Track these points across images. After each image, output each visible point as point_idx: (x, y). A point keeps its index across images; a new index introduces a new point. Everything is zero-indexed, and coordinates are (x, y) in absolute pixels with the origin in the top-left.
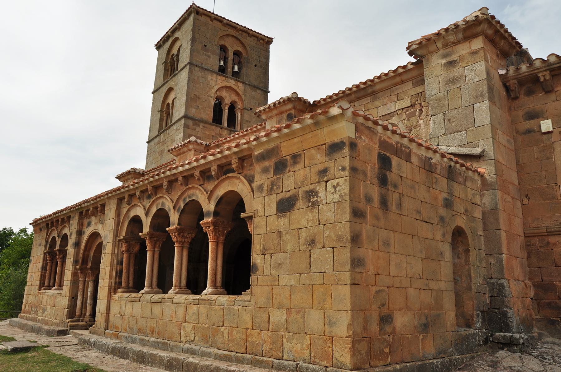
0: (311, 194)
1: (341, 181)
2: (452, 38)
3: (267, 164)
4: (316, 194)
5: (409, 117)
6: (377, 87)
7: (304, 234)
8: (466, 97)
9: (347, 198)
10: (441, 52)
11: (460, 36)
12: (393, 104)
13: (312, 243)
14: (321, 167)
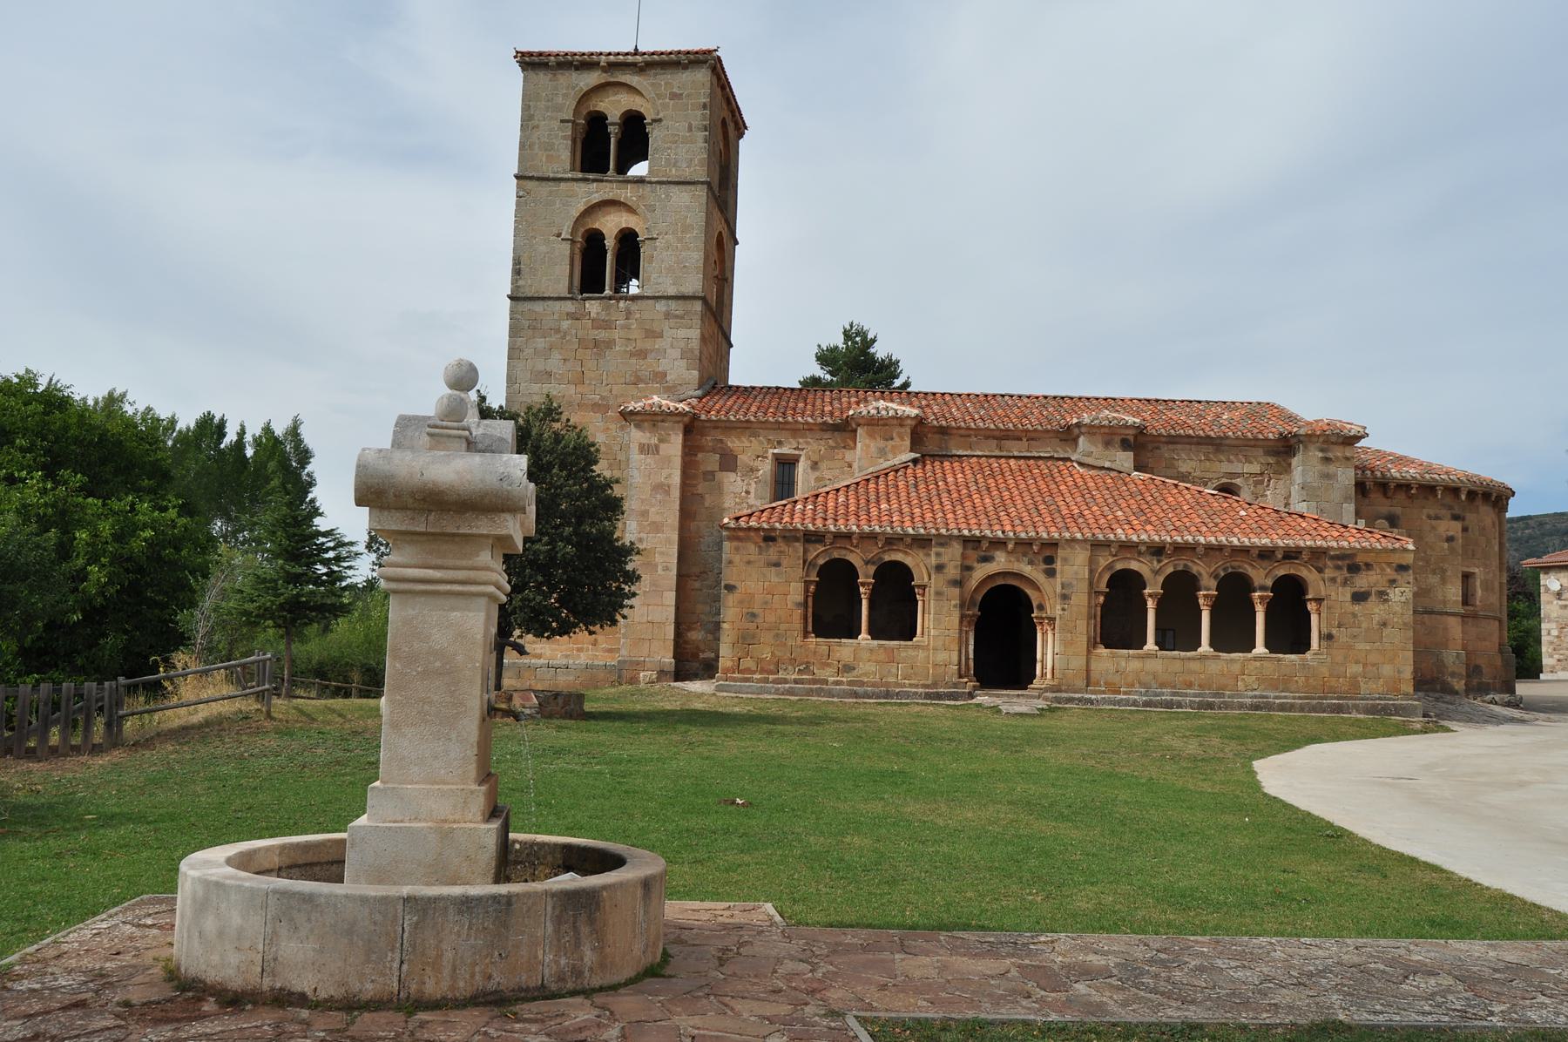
0: (1381, 594)
1: (1407, 590)
2: (1333, 439)
3: (1340, 563)
4: (1387, 594)
5: (1257, 483)
6: (1227, 442)
7: (1376, 619)
8: (1336, 496)
9: (1411, 601)
10: (1318, 444)
11: (1341, 440)
12: (1240, 465)
13: (1384, 624)
14: (1392, 578)
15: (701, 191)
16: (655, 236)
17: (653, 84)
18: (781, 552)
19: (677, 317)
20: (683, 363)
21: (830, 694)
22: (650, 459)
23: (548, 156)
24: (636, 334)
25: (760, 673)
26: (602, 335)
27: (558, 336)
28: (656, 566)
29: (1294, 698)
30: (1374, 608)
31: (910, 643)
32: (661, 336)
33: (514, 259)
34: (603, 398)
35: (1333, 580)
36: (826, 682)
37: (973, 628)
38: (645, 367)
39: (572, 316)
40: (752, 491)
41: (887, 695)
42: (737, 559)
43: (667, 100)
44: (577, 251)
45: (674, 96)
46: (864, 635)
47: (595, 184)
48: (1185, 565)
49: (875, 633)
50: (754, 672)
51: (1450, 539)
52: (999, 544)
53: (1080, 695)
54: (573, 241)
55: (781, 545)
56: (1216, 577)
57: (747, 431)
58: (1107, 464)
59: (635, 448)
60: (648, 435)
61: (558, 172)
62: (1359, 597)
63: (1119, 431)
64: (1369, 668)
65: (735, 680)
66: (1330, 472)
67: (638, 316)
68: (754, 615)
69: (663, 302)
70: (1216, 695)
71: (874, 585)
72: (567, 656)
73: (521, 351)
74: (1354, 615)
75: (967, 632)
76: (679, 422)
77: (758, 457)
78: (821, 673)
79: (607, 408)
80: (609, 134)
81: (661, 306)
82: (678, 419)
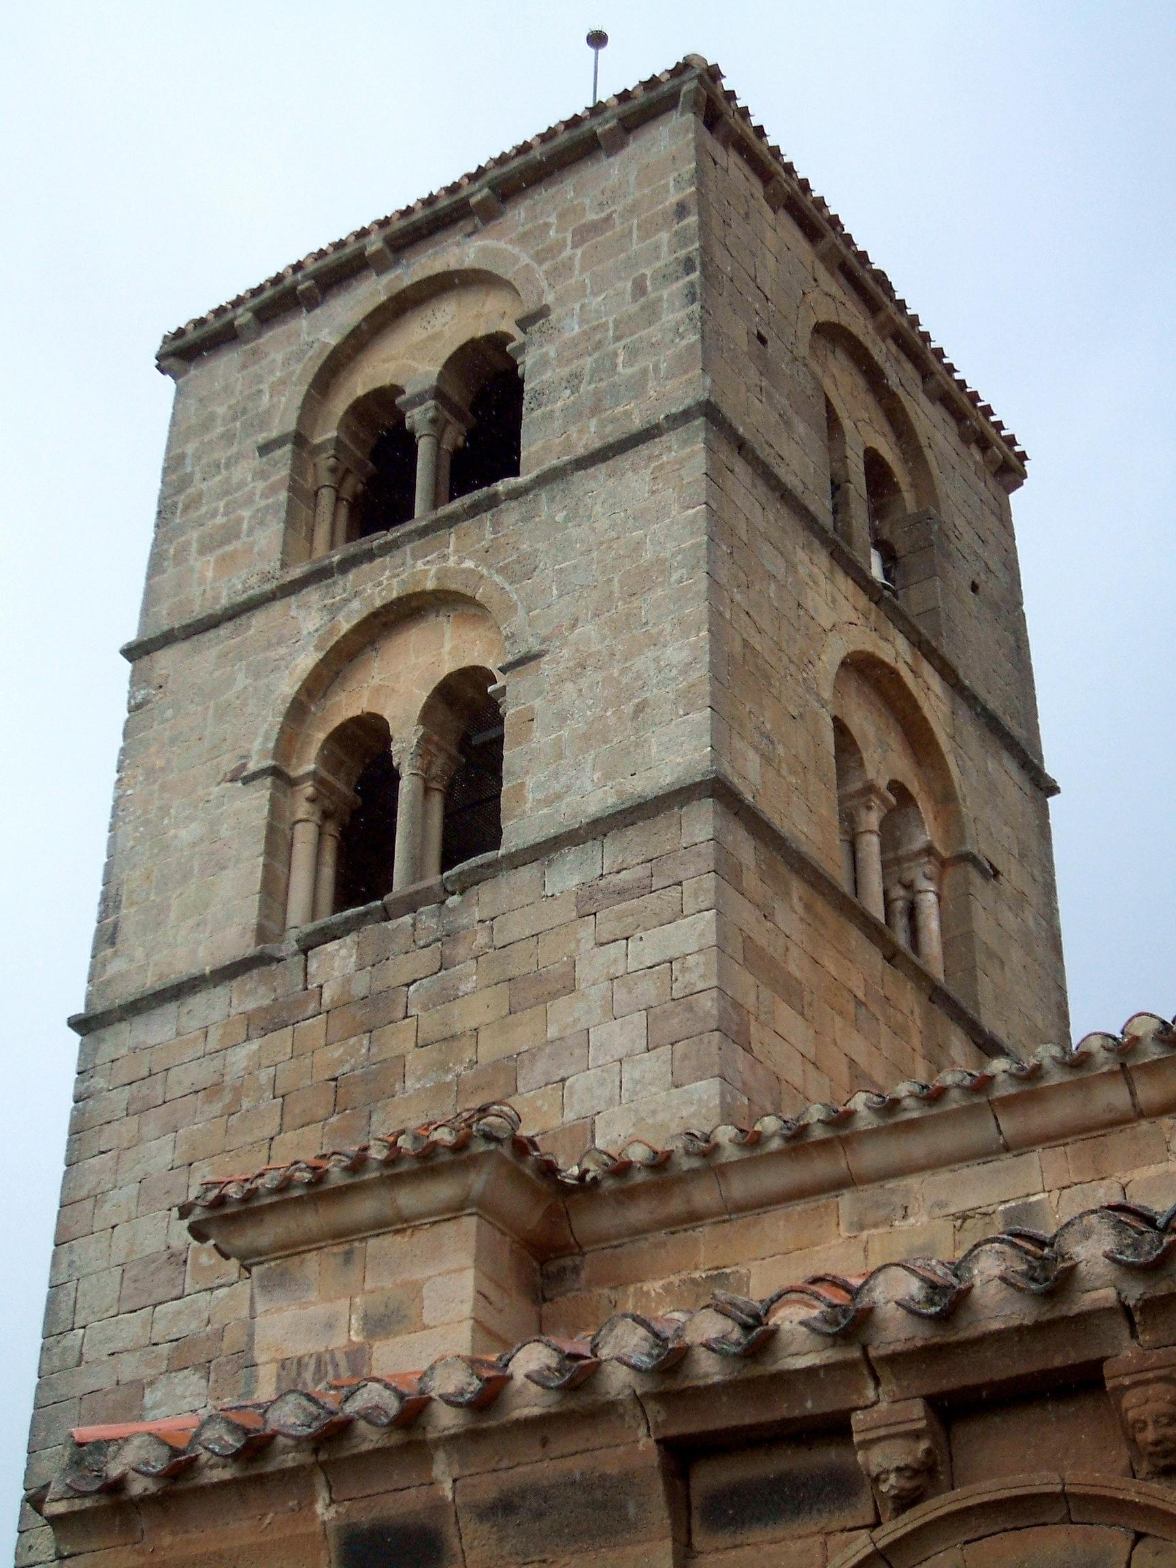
15: (685, 443)
16: (536, 648)
17: (523, 239)
19: (621, 893)
20: (655, 1065)
27: (217, 1108)
32: (569, 986)
33: (104, 898)
44: (303, 809)
45: (584, 233)
54: (279, 775)
57: (846, 1200)
60: (318, 1310)
67: (482, 939)
69: (571, 855)
73: (97, 1198)
76: (455, 1210)
82: (443, 1191)
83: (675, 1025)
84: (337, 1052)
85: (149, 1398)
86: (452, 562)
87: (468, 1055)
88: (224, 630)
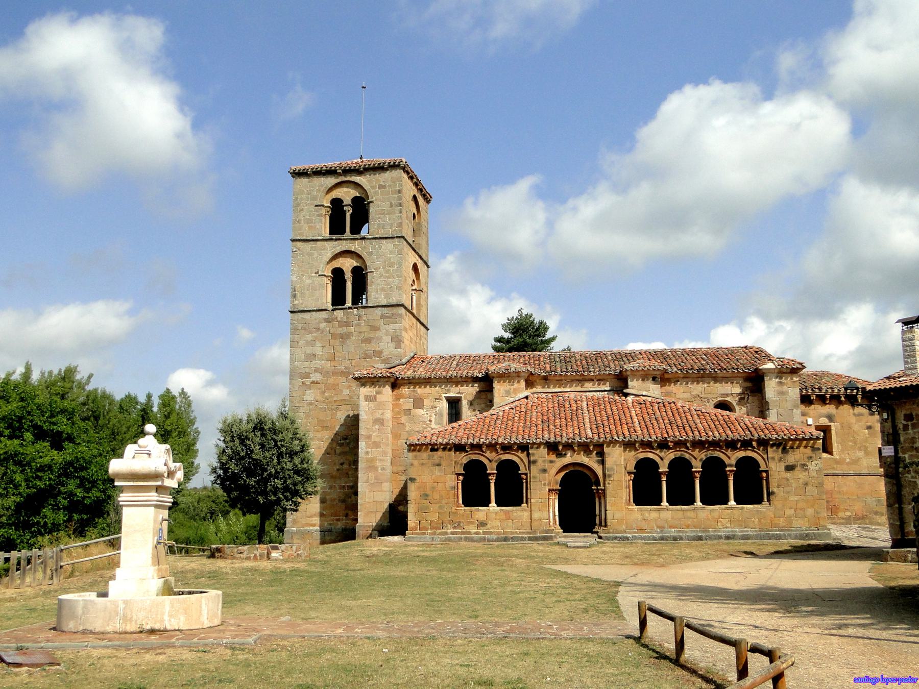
0: (803, 465)
7: (801, 481)
8: (789, 405)
11: (789, 371)
13: (806, 484)
14: (810, 455)
16: (373, 270)
18: (441, 457)
19: (388, 317)
20: (392, 345)
21: (472, 540)
22: (371, 405)
23: (309, 227)
24: (365, 329)
25: (431, 529)
26: (344, 330)
28: (377, 468)
29: (753, 531)
30: (799, 474)
31: (519, 507)
34: (346, 368)
35: (773, 458)
36: (469, 533)
37: (557, 497)
38: (370, 348)
39: (327, 321)
40: (433, 420)
41: (506, 539)
42: (416, 463)
43: (377, 189)
45: (381, 187)
46: (493, 503)
47: (337, 242)
48: (681, 454)
49: (499, 503)
50: (427, 529)
51: (869, 428)
52: (569, 446)
53: (621, 535)
55: (440, 453)
56: (701, 460)
58: (644, 393)
59: (362, 398)
61: (316, 236)
62: (790, 468)
63: (650, 373)
64: (799, 511)
65: (417, 534)
66: (784, 390)
67: (365, 318)
68: (427, 495)
69: (379, 309)
70: (705, 531)
71: (497, 474)
72: (330, 524)
74: (787, 480)
75: (554, 500)
77: (436, 399)
78: (467, 528)
79: (349, 373)
80: (345, 211)
81: (378, 311)
83: (396, 340)
84: (341, 329)
85: (311, 375)
86: (357, 247)
87: (363, 335)
88: (312, 243)
